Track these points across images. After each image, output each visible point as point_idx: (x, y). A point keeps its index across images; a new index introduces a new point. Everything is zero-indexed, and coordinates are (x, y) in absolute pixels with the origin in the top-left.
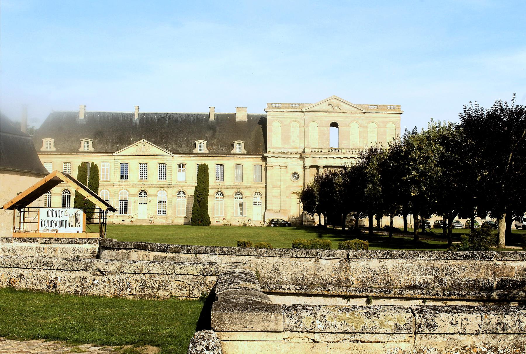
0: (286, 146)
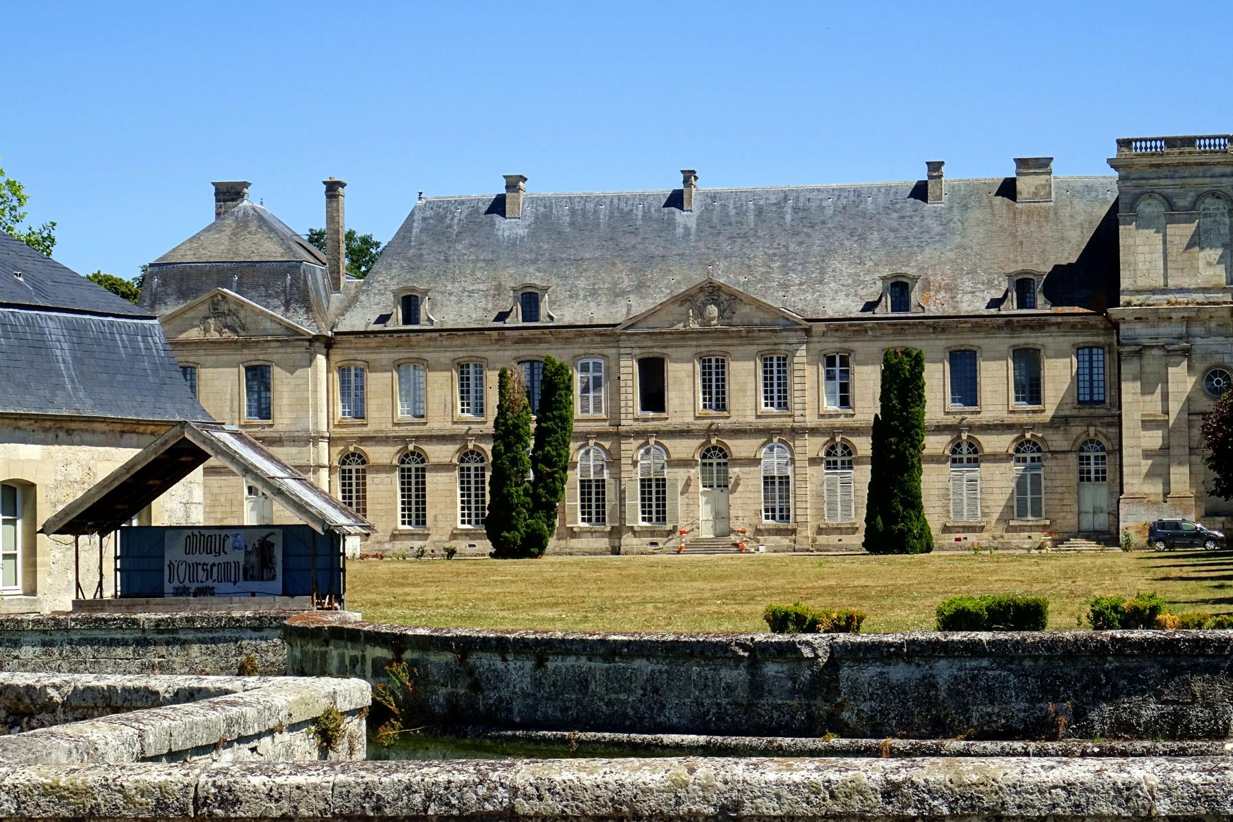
0: (1187, 282)
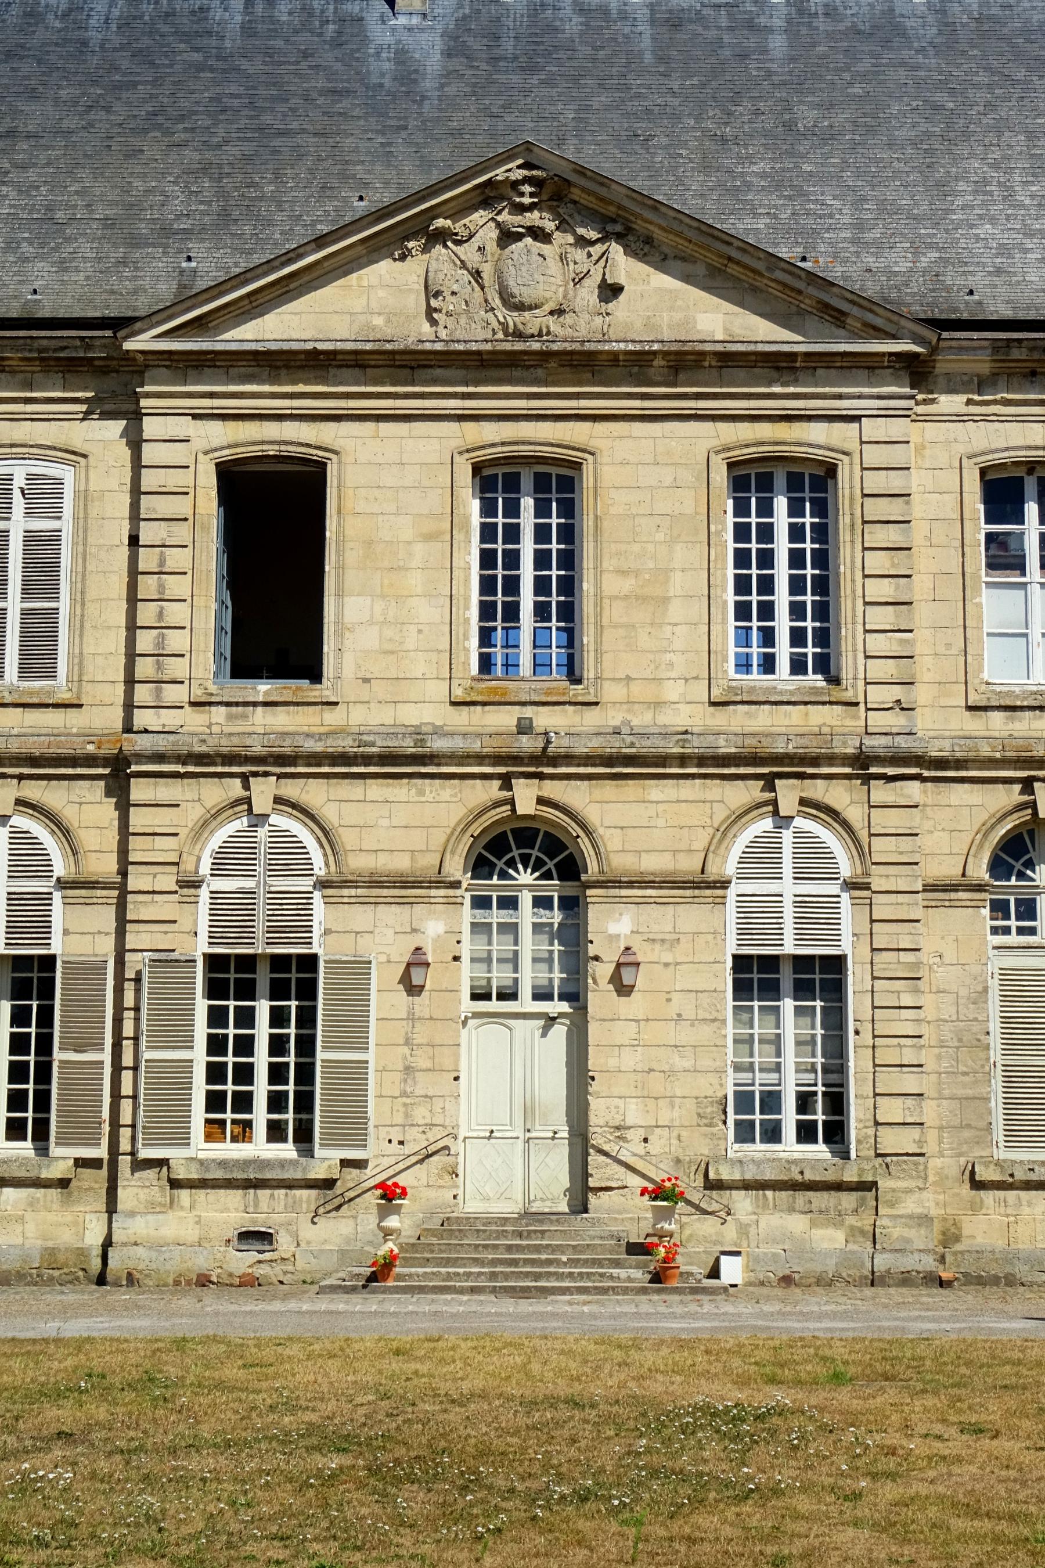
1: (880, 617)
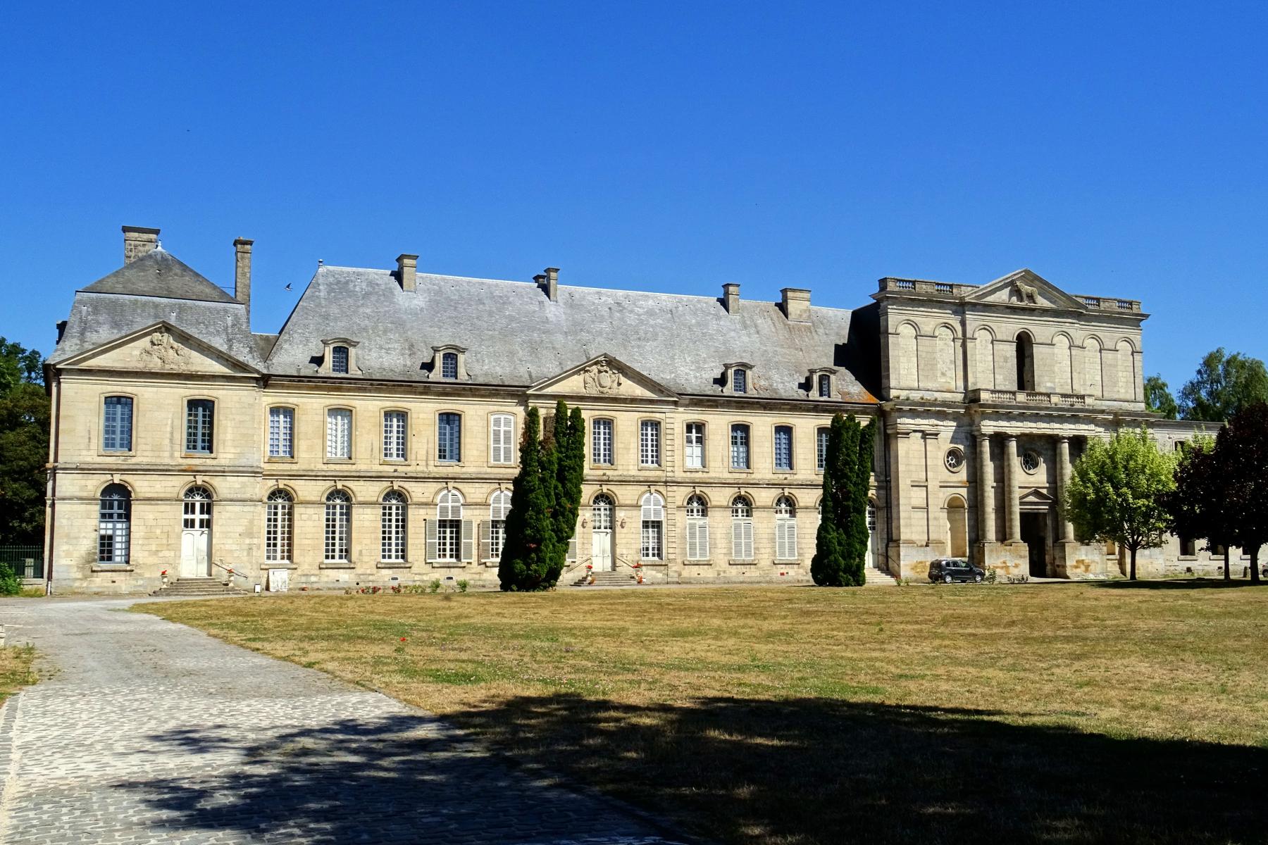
0: (930, 385)
1: (669, 453)
